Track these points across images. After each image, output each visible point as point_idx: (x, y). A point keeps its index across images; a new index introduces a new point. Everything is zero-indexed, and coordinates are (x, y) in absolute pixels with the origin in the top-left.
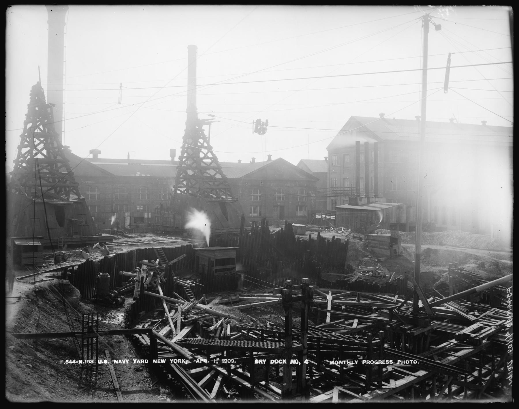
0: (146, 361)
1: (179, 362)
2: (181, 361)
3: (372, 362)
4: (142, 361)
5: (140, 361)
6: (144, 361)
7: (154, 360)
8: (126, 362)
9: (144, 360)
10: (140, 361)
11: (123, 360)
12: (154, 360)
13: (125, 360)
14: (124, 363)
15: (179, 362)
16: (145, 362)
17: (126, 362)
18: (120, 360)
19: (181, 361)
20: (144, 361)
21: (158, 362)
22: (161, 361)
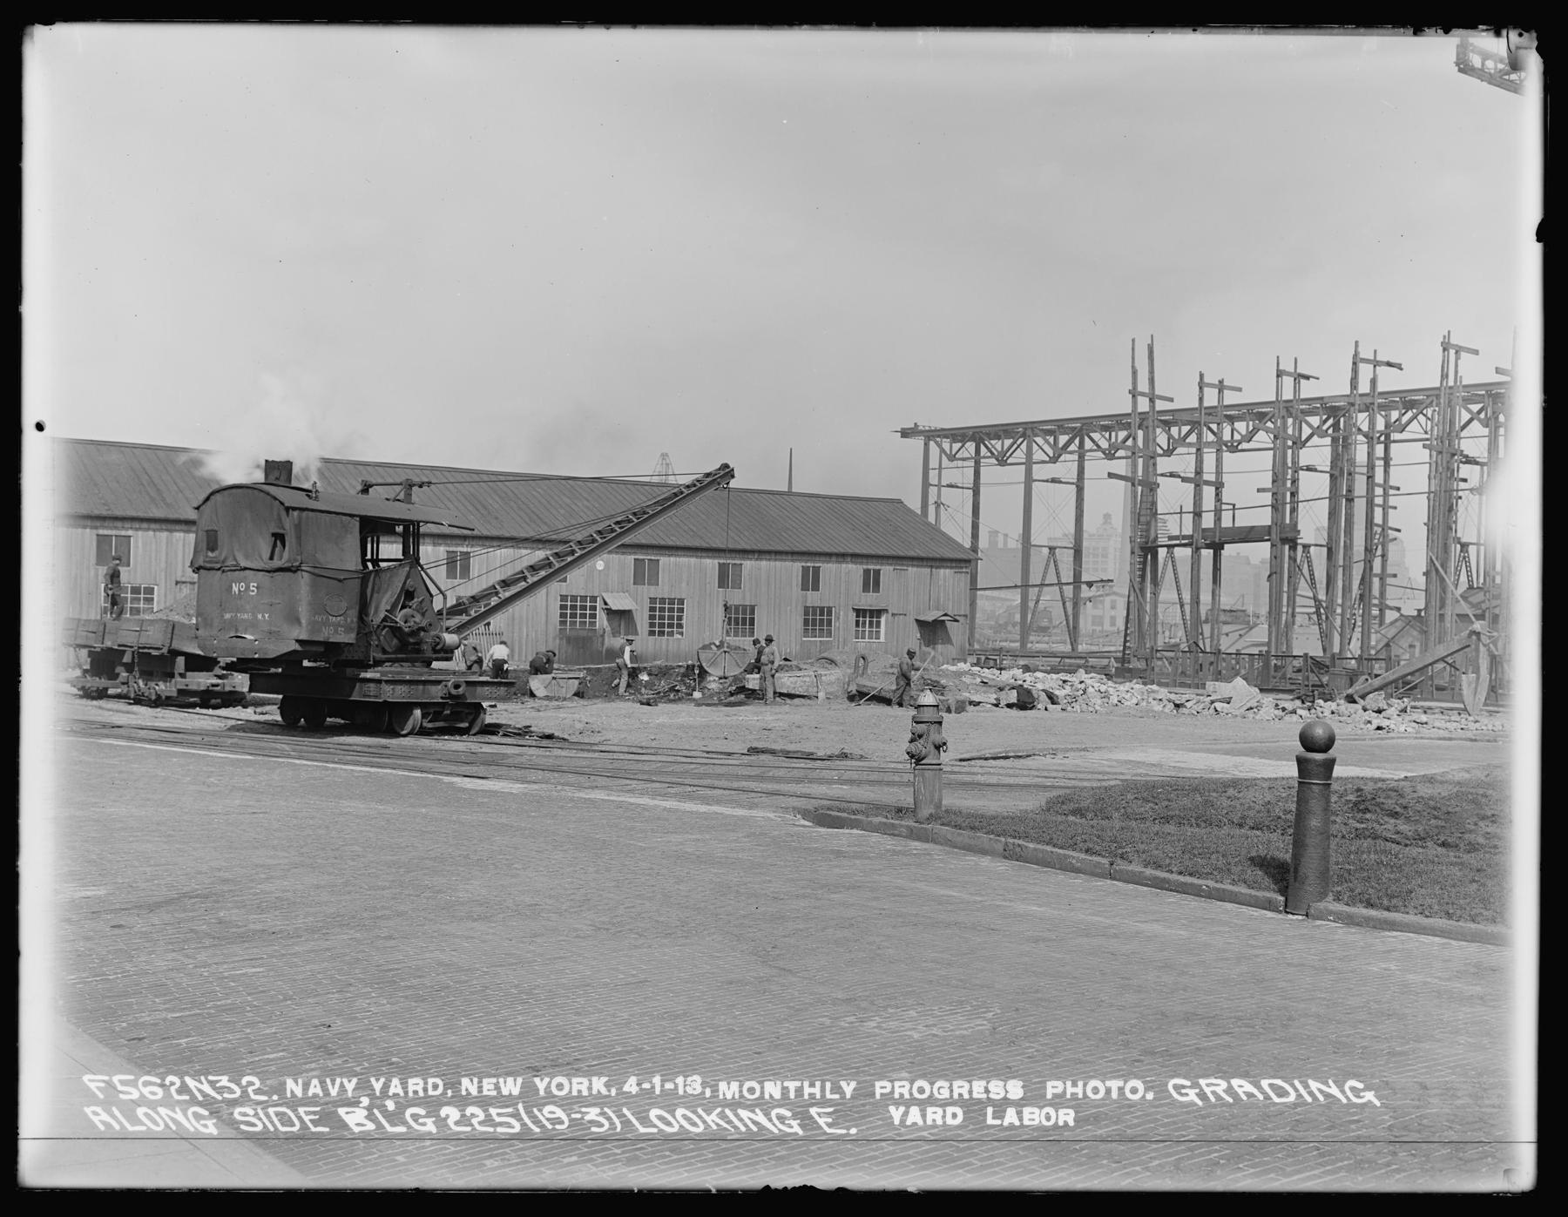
0: (435, 1087)
2: (590, 1089)
3: (921, 1091)
4: (411, 1089)
6: (425, 1090)
7: (465, 1082)
9: (421, 1083)
11: (328, 1081)
12: (465, 1082)
13: (338, 1081)
14: (334, 1092)
15: (579, 1091)
16: (431, 1092)
19: (590, 1089)
20: (425, 1090)
22: (497, 1087)
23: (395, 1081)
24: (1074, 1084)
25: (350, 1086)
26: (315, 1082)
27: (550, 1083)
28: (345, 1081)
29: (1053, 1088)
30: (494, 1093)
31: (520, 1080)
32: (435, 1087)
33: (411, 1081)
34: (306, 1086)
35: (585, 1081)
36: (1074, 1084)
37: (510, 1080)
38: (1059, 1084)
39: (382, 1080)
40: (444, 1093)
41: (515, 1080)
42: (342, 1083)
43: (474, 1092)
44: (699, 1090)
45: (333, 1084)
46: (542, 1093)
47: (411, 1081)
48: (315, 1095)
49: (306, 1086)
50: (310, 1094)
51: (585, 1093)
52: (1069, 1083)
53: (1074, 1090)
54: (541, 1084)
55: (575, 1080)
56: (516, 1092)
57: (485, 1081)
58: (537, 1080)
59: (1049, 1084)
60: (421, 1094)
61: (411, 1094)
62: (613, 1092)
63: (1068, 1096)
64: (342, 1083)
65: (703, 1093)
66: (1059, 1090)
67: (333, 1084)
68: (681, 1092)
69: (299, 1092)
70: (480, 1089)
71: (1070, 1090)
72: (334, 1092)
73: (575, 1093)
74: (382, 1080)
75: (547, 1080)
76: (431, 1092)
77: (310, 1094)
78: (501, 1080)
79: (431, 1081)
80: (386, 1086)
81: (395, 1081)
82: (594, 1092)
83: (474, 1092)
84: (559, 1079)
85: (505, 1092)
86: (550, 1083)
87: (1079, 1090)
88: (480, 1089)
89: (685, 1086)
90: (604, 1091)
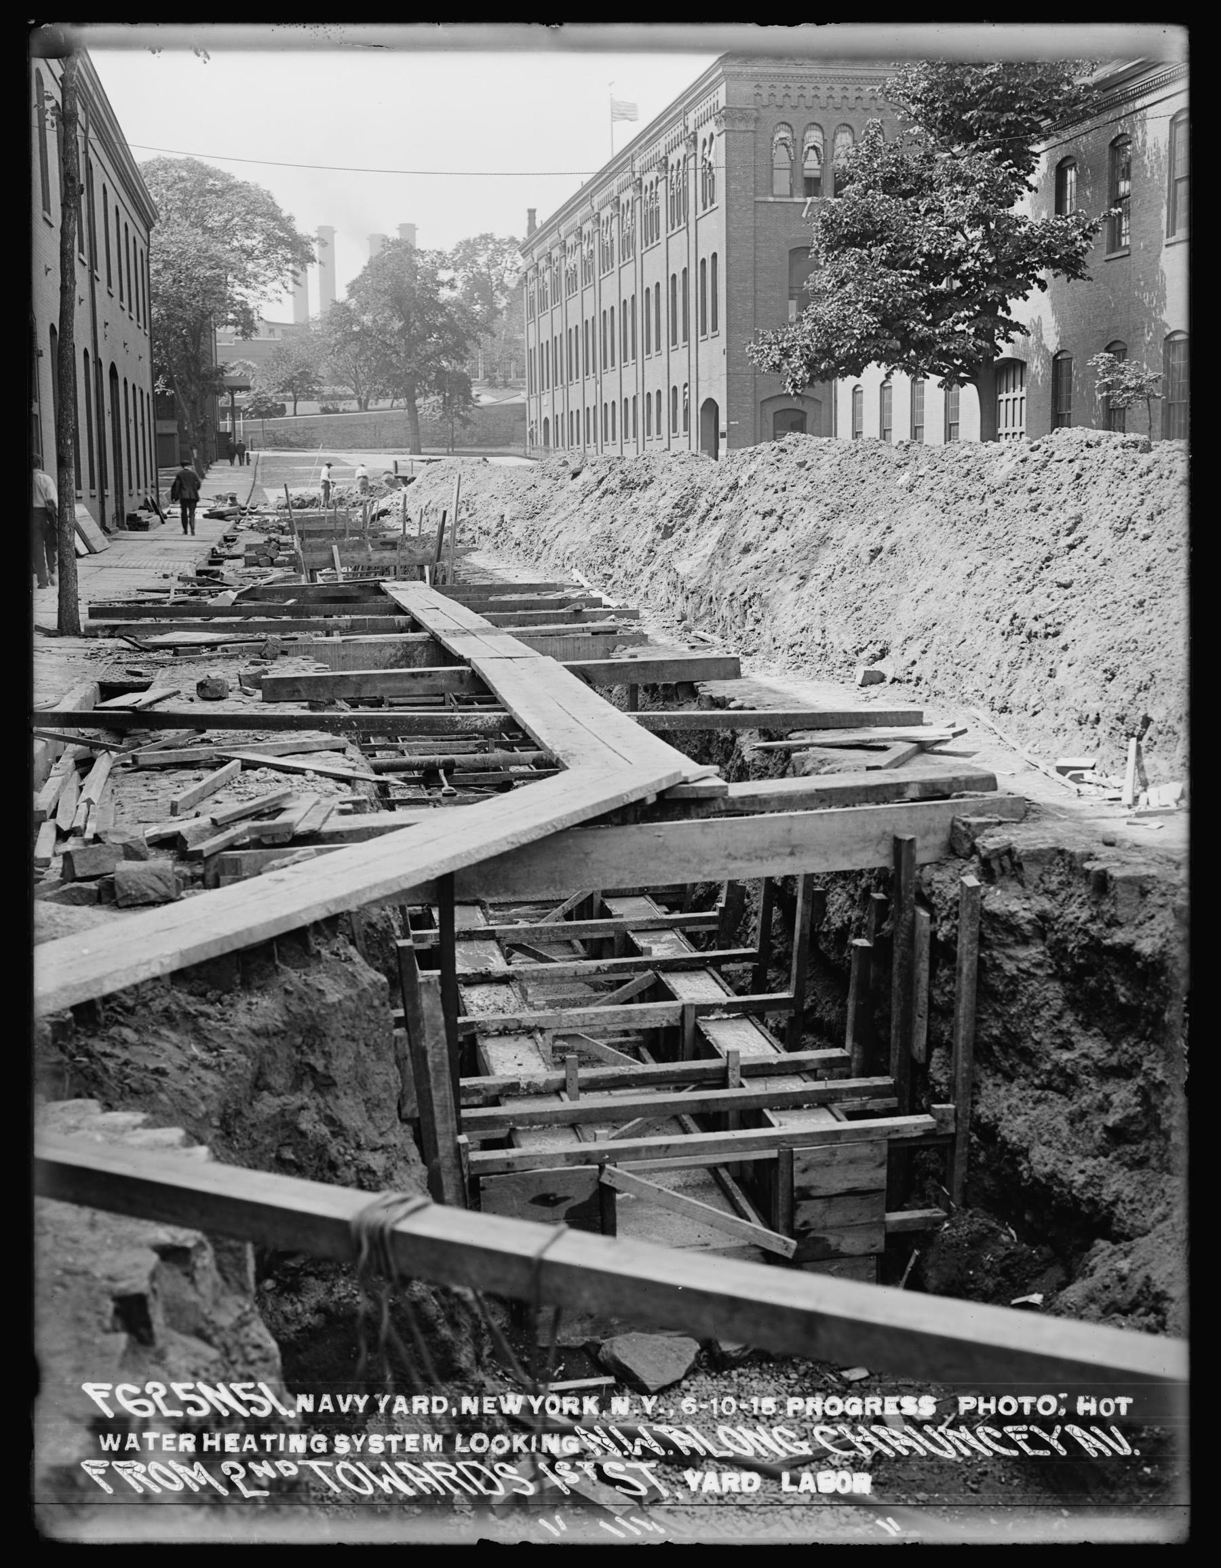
5: (410, 1405)
6: (430, 1407)
8: (353, 1406)
10: (410, 1405)
11: (340, 1398)
14: (345, 1409)
17: (353, 1406)
18: (326, 1398)
20: (430, 1407)
21: (486, 1411)
24: (987, 1401)
25: (361, 1402)
26: (326, 1398)
28: (357, 1398)
29: (966, 1403)
32: (440, 1404)
33: (416, 1399)
34: (317, 1404)
36: (987, 1401)
37: (511, 1397)
38: (973, 1401)
39: (387, 1398)
43: (474, 1411)
46: (536, 1412)
48: (326, 1411)
49: (317, 1404)
52: (981, 1399)
53: (987, 1406)
54: (536, 1404)
57: (486, 1399)
59: (962, 1400)
60: (425, 1411)
61: (415, 1411)
63: (981, 1411)
66: (971, 1407)
69: (310, 1408)
70: (481, 1406)
71: (982, 1406)
72: (345, 1409)
75: (541, 1398)
78: (502, 1398)
79: (435, 1399)
83: (474, 1411)
87: (991, 1406)
88: (481, 1406)
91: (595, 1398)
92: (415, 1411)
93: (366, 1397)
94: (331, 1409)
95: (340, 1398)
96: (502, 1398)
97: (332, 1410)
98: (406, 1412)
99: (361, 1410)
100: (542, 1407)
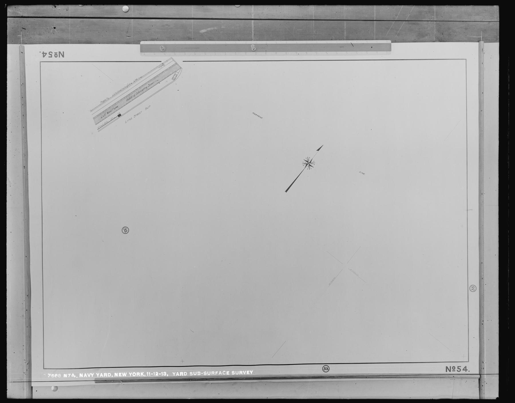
0: (109, 375)
1: (138, 375)
2: (140, 374)
5: (103, 375)
6: (107, 375)
8: (91, 375)
10: (103, 375)
11: (88, 374)
13: (90, 374)
14: (89, 376)
15: (138, 375)
16: (108, 376)
17: (91, 375)
18: (85, 374)
19: (140, 374)
20: (107, 375)
21: (119, 376)
22: (122, 374)
23: (101, 374)
25: (92, 375)
26: (85, 374)
27: (132, 374)
28: (91, 374)
30: (121, 376)
31: (126, 373)
32: (109, 375)
33: (104, 374)
34: (84, 375)
35: (139, 373)
37: (124, 373)
39: (99, 374)
40: (111, 375)
41: (125, 373)
42: (91, 375)
43: (117, 376)
44: (166, 375)
45: (89, 375)
46: (131, 375)
47: (104, 374)
48: (86, 377)
49: (84, 375)
50: (84, 377)
51: (139, 375)
55: (137, 373)
56: (125, 375)
58: (130, 373)
61: (104, 376)
62: (145, 375)
64: (91, 375)
65: (167, 375)
67: (89, 375)
68: (162, 375)
69: (82, 376)
72: (89, 376)
73: (137, 375)
74: (99, 374)
75: (132, 373)
76: (108, 376)
77: (84, 377)
79: (108, 374)
80: (99, 375)
81: (101, 374)
82: (141, 375)
84: (134, 373)
85: (123, 376)
86: (132, 374)
89: (163, 374)
90: (143, 375)
91: (143, 373)
92: (104, 376)
93: (93, 374)
94: (87, 376)
95: (88, 374)
96: (122, 373)
97: (87, 376)
98: (103, 376)
99: (92, 376)
100: (132, 374)
